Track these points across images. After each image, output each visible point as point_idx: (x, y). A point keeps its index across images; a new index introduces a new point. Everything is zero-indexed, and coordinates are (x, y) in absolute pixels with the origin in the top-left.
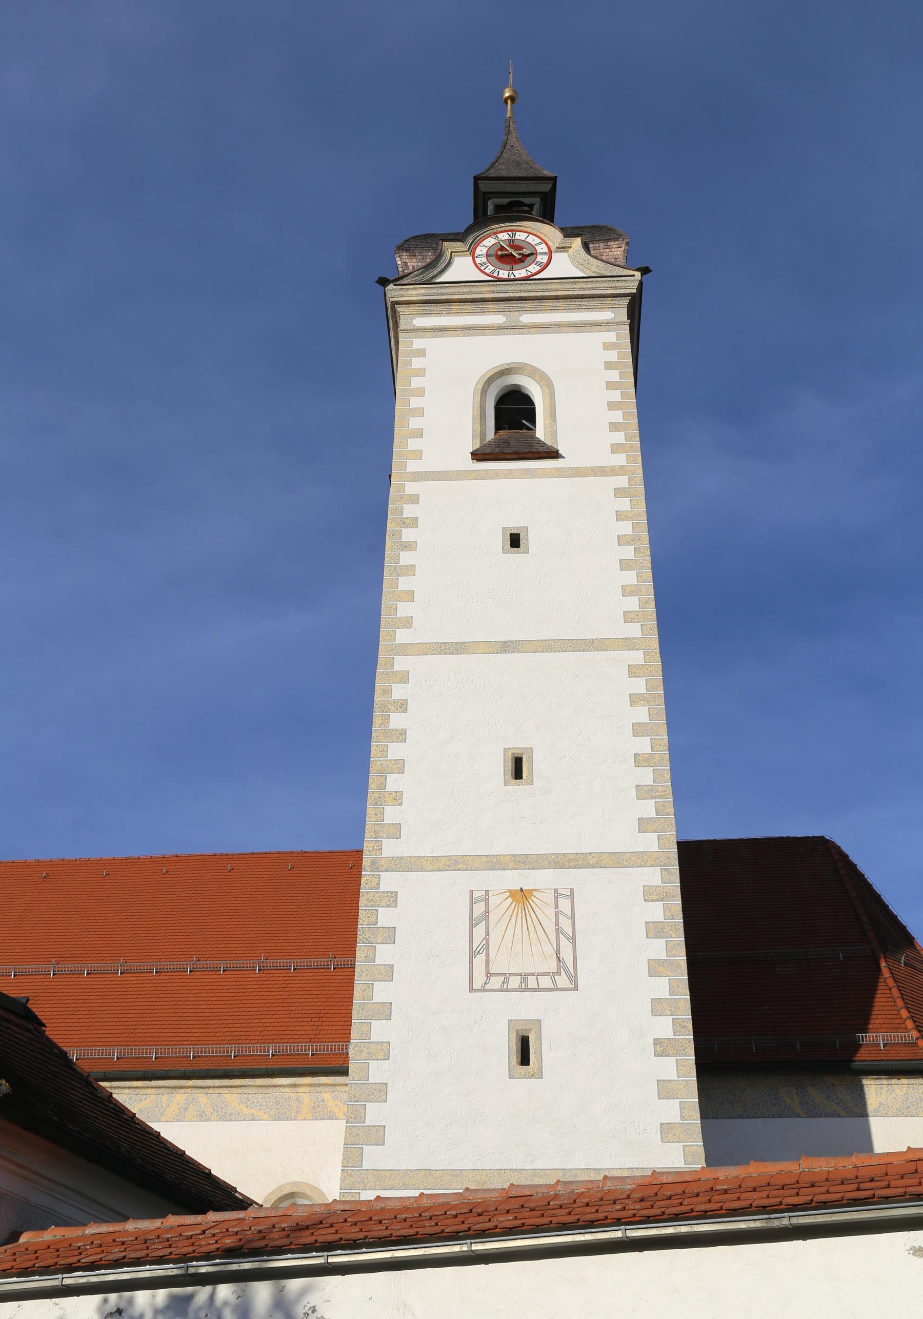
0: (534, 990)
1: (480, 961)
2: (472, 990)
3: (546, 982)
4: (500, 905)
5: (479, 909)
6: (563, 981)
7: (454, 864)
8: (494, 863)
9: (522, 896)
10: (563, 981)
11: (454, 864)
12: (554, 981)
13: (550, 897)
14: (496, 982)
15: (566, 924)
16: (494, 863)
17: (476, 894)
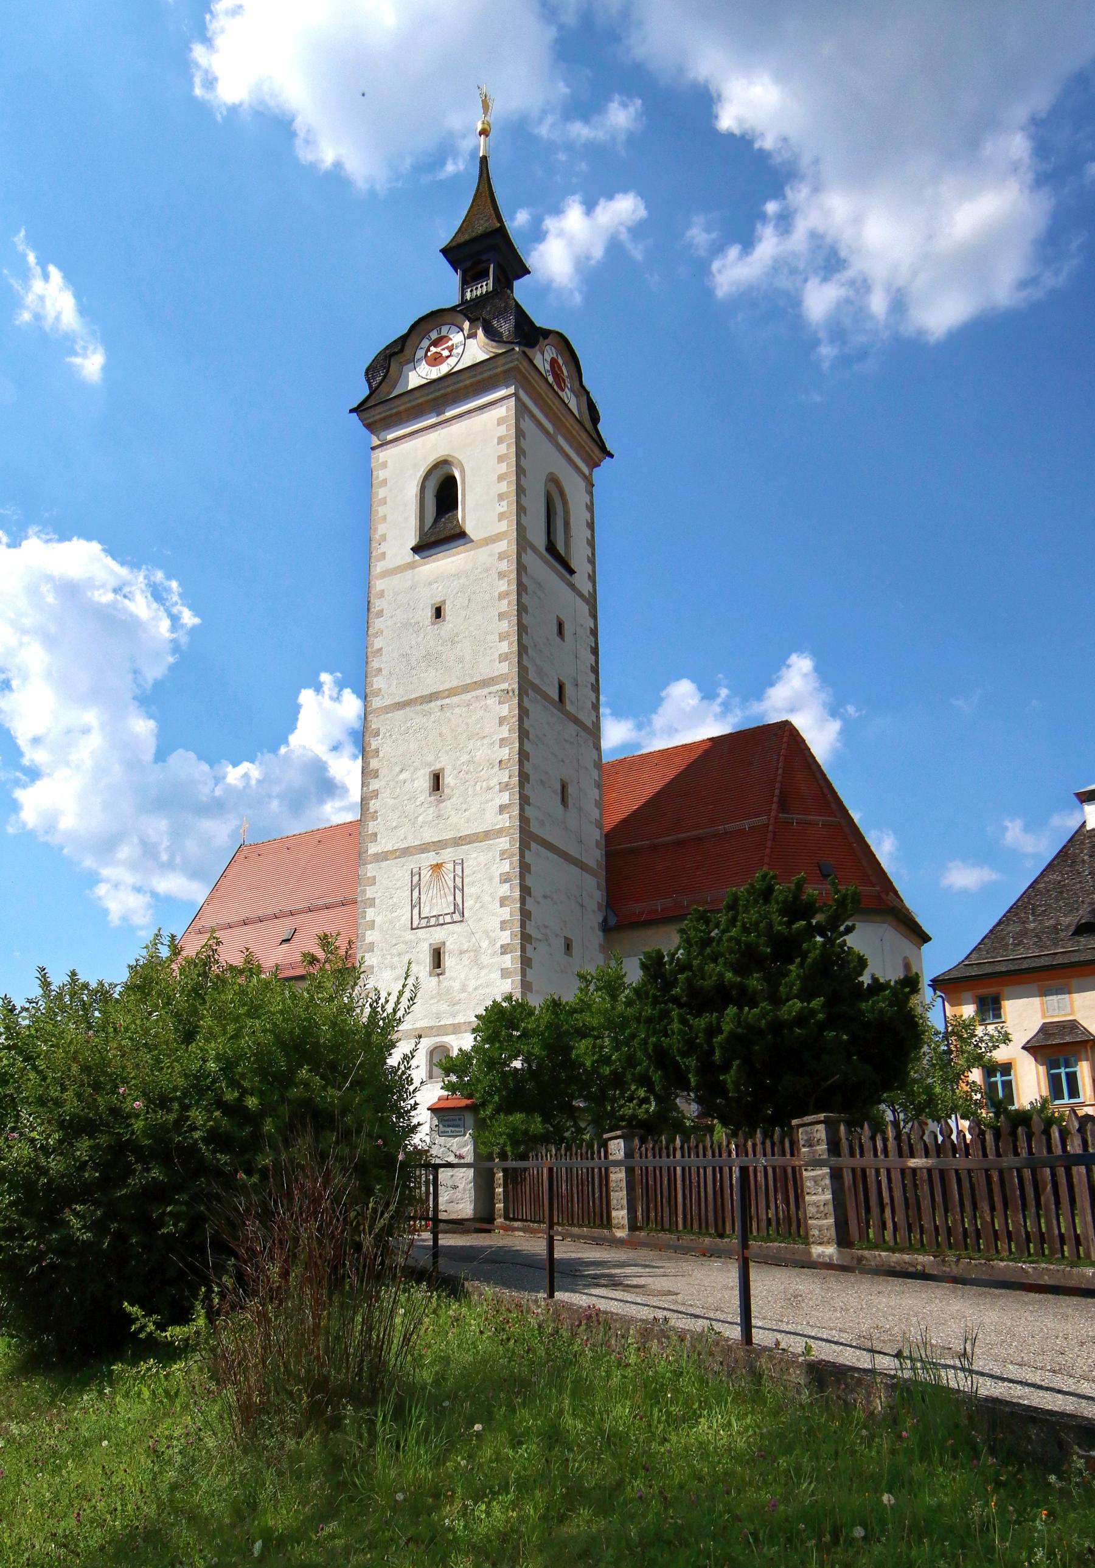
0: (442, 924)
1: (416, 911)
2: (412, 929)
3: (448, 919)
4: (426, 874)
5: (416, 879)
6: (457, 917)
7: (406, 852)
8: (424, 848)
9: (437, 867)
10: (457, 917)
11: (406, 852)
12: (452, 917)
13: (450, 866)
14: (424, 923)
15: (458, 881)
16: (424, 848)
17: (414, 871)
